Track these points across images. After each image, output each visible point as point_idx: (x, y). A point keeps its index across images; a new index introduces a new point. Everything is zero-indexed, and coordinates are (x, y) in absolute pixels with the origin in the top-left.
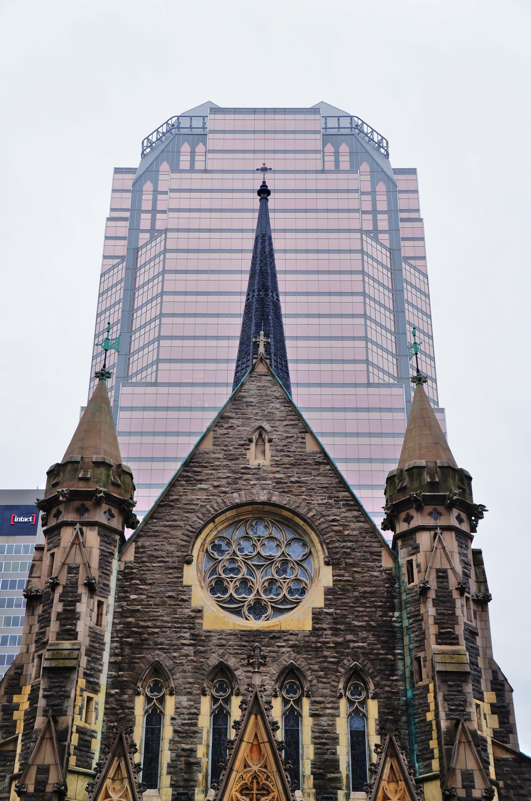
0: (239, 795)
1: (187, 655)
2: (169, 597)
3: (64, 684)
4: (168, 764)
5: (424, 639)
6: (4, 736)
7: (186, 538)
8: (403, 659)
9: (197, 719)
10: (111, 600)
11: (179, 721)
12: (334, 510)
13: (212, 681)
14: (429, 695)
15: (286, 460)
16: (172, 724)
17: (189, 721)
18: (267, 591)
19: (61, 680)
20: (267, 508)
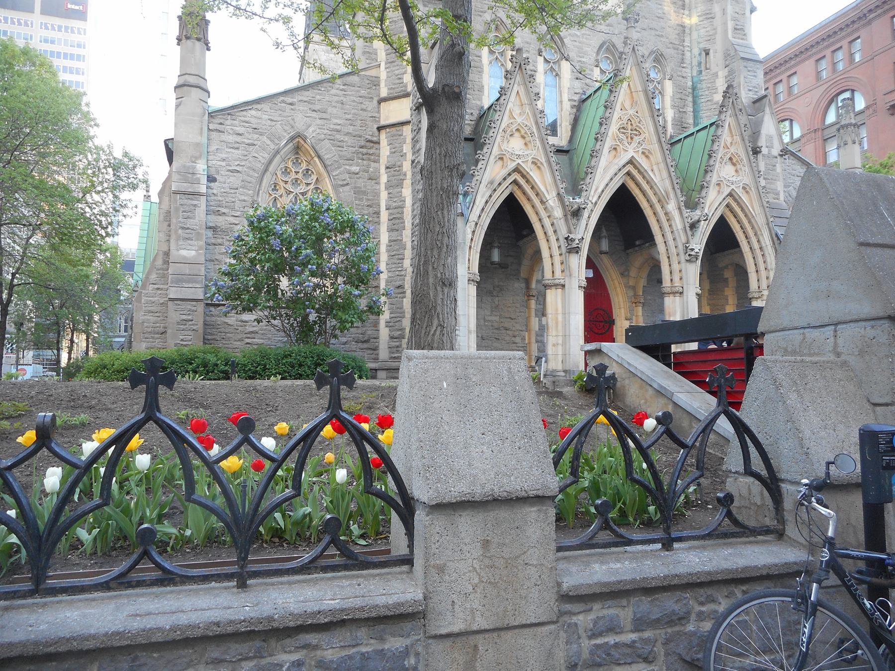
5: (716, 33)
6: (368, 61)
8: (691, 51)
14: (717, 80)
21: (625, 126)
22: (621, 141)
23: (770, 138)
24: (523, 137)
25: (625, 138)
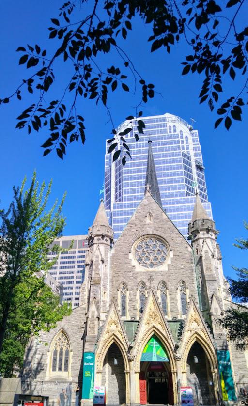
10: (109, 265)
12: (173, 235)
15: (157, 221)
18: (154, 260)
22: (150, 320)
23: (216, 309)
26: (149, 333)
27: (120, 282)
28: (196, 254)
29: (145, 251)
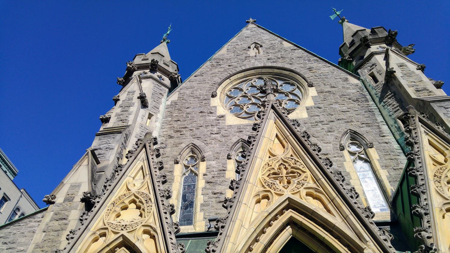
0: (267, 179)
1: (215, 138)
2: (201, 112)
3: (110, 142)
4: (201, 204)
7: (211, 87)
9: (225, 173)
11: (210, 176)
13: (235, 151)
16: (204, 178)
17: (219, 175)
19: (109, 140)
20: (264, 70)
21: (276, 170)
24: (138, 208)
25: (278, 182)
26: (270, 231)
27: (183, 145)
28: (372, 83)
29: (249, 95)
